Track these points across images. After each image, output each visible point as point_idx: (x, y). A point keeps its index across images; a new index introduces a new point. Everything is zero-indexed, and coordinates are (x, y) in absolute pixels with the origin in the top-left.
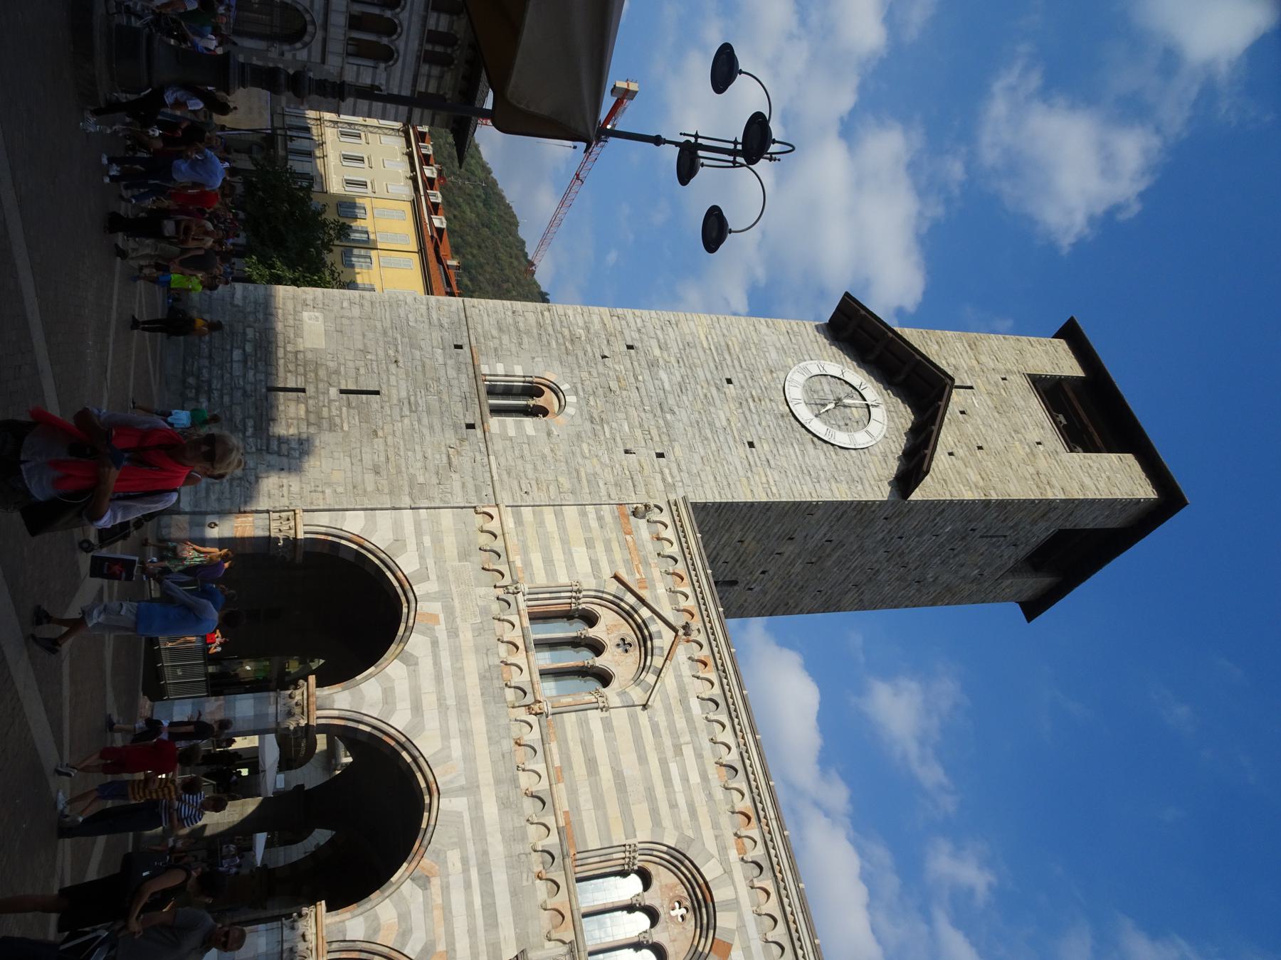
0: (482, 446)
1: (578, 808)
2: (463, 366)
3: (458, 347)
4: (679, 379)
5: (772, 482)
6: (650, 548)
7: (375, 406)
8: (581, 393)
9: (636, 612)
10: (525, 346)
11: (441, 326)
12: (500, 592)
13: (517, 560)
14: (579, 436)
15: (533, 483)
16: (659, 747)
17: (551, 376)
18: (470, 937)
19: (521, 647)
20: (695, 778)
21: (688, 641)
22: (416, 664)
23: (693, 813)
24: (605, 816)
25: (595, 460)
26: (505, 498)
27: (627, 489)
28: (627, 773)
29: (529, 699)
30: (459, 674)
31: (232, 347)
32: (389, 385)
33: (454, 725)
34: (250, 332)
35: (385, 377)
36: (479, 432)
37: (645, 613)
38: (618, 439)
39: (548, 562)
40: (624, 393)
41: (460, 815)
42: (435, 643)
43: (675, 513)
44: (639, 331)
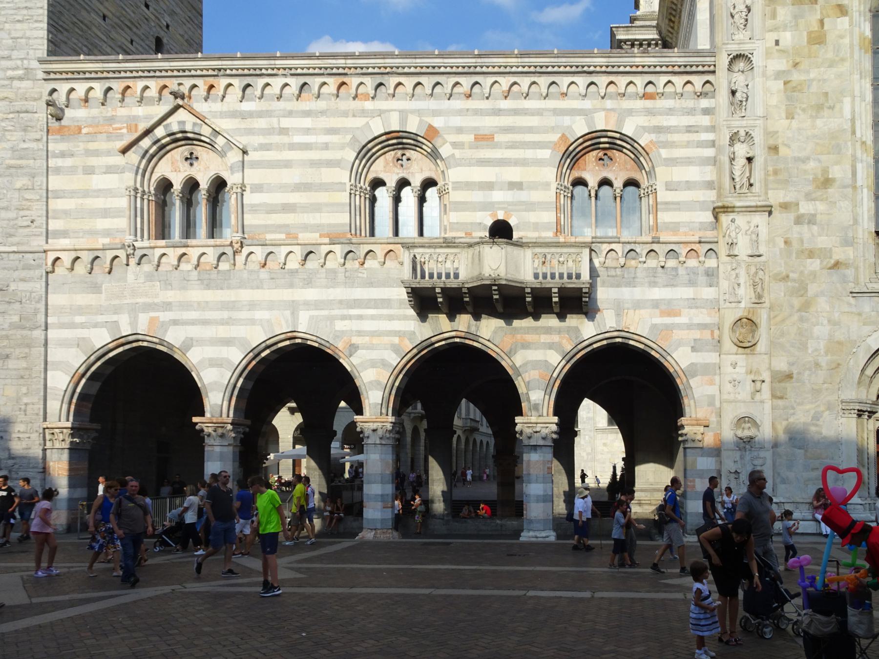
1: (319, 226)
6: (94, 111)
9: (159, 140)
12: (133, 261)
15: (22, 213)
16: (280, 147)
18: (393, 319)
19: (183, 250)
20: (307, 122)
21: (190, 98)
24: (327, 205)
26: (38, 243)
27: (31, 120)
29: (229, 251)
37: (160, 132)
39: (106, 213)
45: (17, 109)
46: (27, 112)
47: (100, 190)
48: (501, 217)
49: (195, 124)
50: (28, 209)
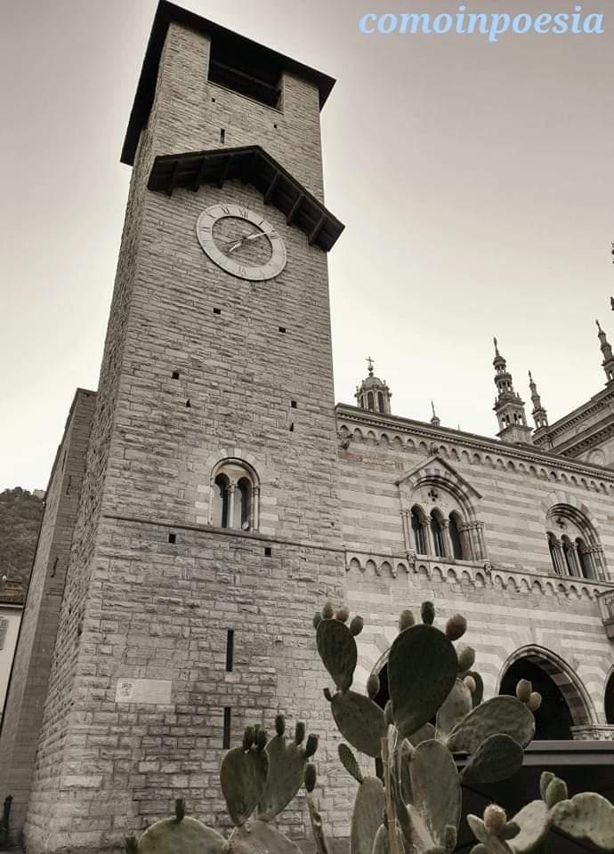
0: (289, 547)
2: (200, 541)
3: (172, 539)
4: (215, 351)
5: (316, 334)
6: (371, 448)
7: (250, 637)
8: (233, 442)
10: (175, 472)
11: (141, 549)
13: (387, 550)
14: (278, 462)
15: (323, 515)
16: (499, 500)
17: (212, 461)
19: (451, 567)
20: (513, 487)
23: (529, 496)
25: (301, 458)
28: (514, 526)
31: (168, 788)
32: (223, 619)
33: (497, 626)
34: (144, 767)
35: (211, 623)
36: (274, 546)
38: (281, 431)
39: (386, 527)
40: (231, 405)
41: (544, 634)
43: (352, 419)
44: (155, 358)
45: (316, 433)
46: (323, 437)
47: (379, 508)
50: (328, 513)
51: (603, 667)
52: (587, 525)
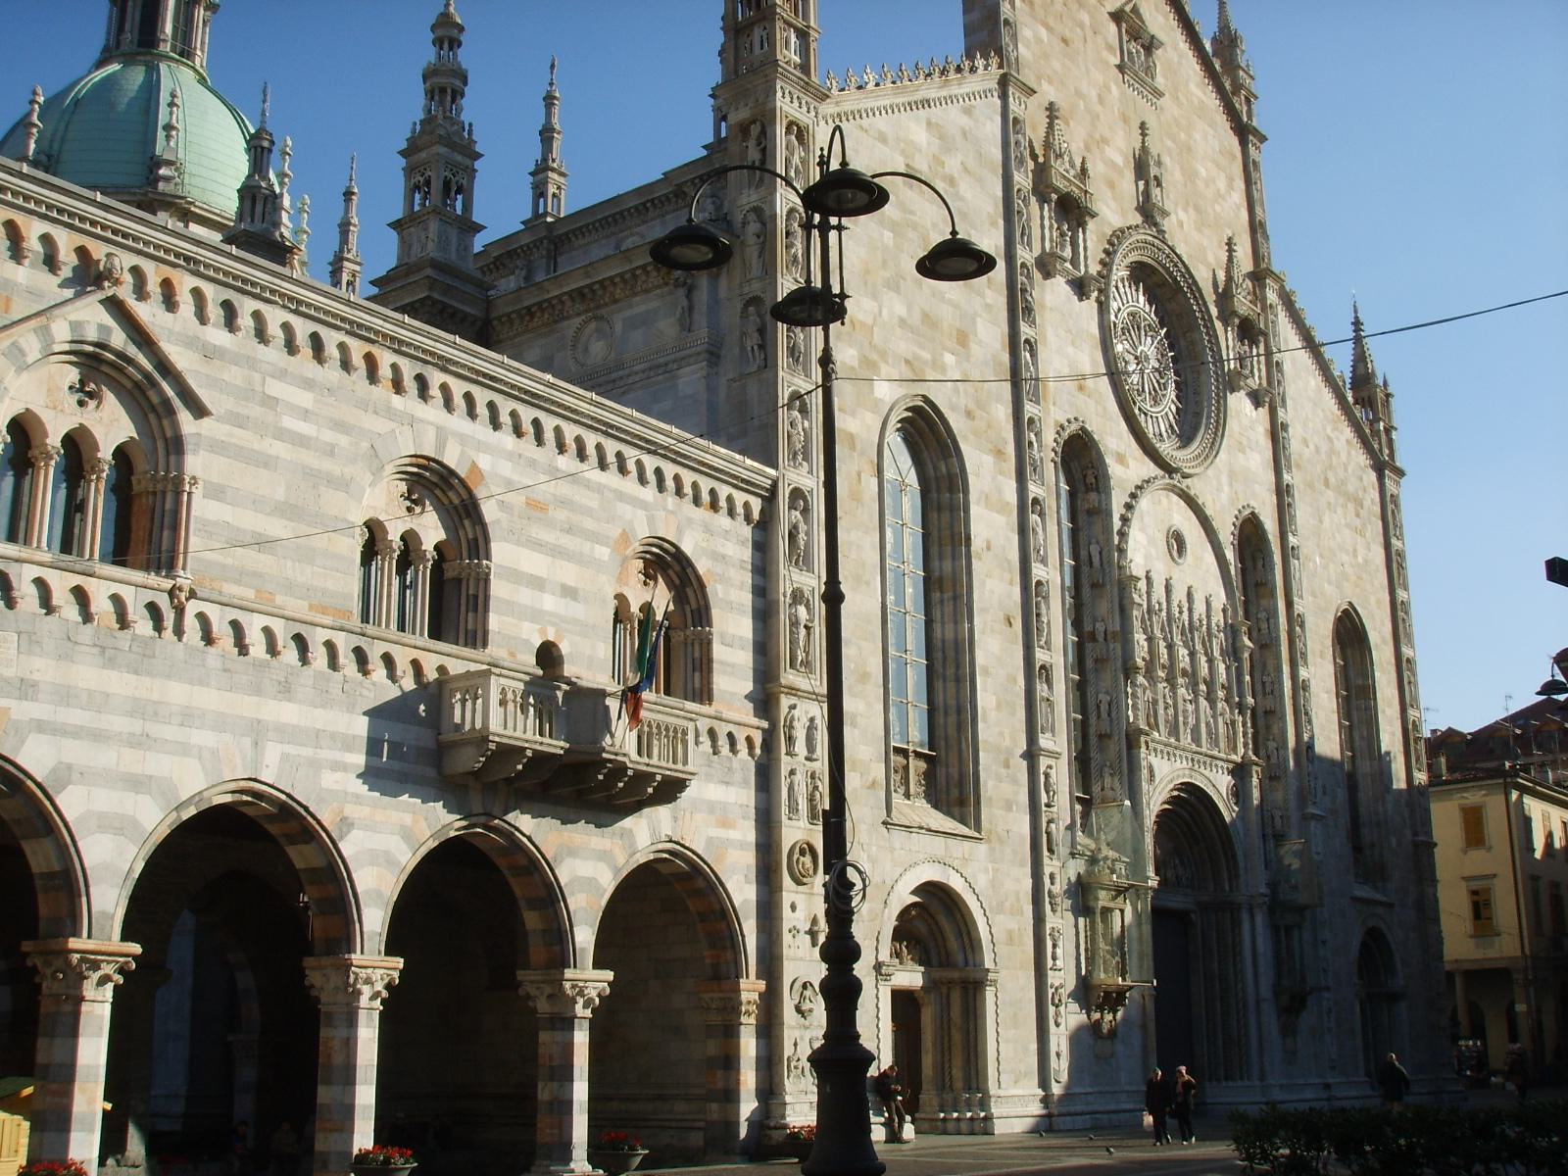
20: (305, 399)
22: (69, 767)
28: (280, 494)
30: (100, 701)
33: (170, 732)
41: (285, 757)
42: (41, 727)
48: (551, 639)
49: (102, 328)
51: (406, 834)
52: (469, 516)
